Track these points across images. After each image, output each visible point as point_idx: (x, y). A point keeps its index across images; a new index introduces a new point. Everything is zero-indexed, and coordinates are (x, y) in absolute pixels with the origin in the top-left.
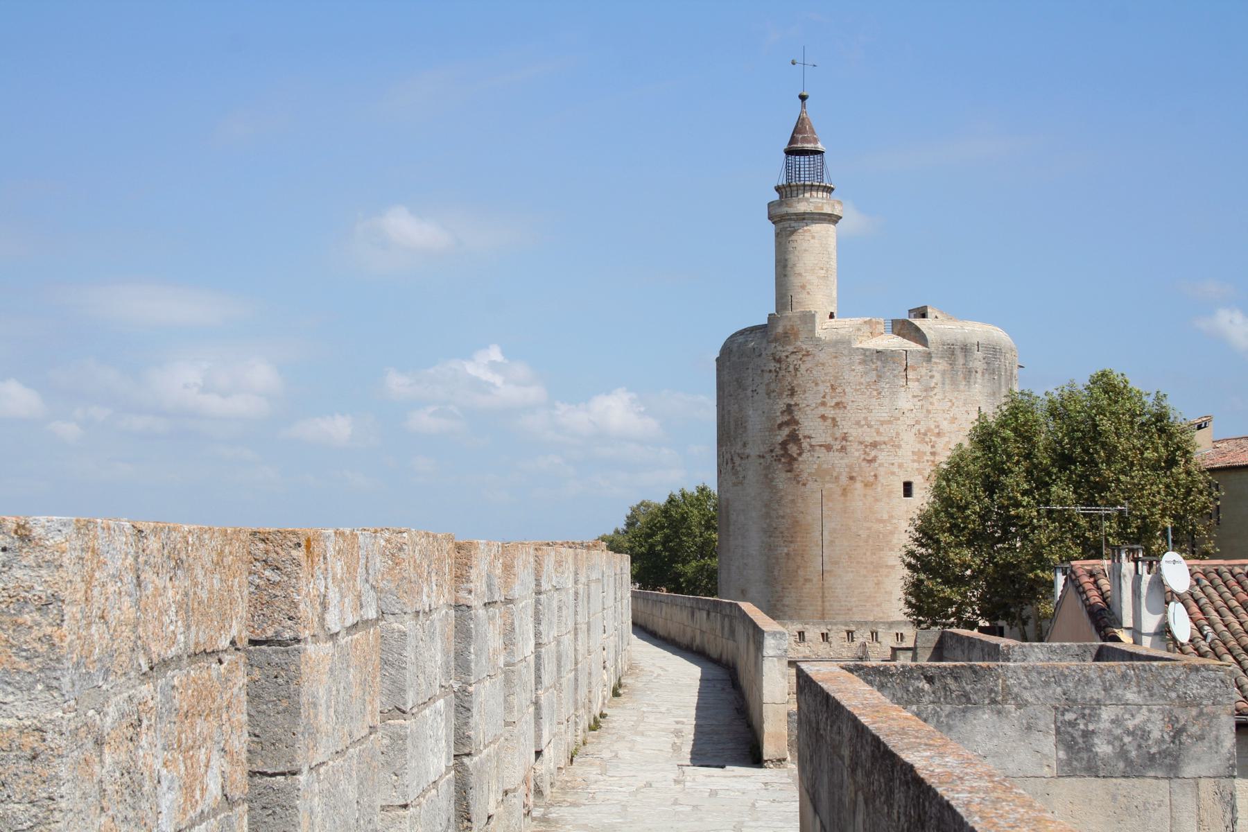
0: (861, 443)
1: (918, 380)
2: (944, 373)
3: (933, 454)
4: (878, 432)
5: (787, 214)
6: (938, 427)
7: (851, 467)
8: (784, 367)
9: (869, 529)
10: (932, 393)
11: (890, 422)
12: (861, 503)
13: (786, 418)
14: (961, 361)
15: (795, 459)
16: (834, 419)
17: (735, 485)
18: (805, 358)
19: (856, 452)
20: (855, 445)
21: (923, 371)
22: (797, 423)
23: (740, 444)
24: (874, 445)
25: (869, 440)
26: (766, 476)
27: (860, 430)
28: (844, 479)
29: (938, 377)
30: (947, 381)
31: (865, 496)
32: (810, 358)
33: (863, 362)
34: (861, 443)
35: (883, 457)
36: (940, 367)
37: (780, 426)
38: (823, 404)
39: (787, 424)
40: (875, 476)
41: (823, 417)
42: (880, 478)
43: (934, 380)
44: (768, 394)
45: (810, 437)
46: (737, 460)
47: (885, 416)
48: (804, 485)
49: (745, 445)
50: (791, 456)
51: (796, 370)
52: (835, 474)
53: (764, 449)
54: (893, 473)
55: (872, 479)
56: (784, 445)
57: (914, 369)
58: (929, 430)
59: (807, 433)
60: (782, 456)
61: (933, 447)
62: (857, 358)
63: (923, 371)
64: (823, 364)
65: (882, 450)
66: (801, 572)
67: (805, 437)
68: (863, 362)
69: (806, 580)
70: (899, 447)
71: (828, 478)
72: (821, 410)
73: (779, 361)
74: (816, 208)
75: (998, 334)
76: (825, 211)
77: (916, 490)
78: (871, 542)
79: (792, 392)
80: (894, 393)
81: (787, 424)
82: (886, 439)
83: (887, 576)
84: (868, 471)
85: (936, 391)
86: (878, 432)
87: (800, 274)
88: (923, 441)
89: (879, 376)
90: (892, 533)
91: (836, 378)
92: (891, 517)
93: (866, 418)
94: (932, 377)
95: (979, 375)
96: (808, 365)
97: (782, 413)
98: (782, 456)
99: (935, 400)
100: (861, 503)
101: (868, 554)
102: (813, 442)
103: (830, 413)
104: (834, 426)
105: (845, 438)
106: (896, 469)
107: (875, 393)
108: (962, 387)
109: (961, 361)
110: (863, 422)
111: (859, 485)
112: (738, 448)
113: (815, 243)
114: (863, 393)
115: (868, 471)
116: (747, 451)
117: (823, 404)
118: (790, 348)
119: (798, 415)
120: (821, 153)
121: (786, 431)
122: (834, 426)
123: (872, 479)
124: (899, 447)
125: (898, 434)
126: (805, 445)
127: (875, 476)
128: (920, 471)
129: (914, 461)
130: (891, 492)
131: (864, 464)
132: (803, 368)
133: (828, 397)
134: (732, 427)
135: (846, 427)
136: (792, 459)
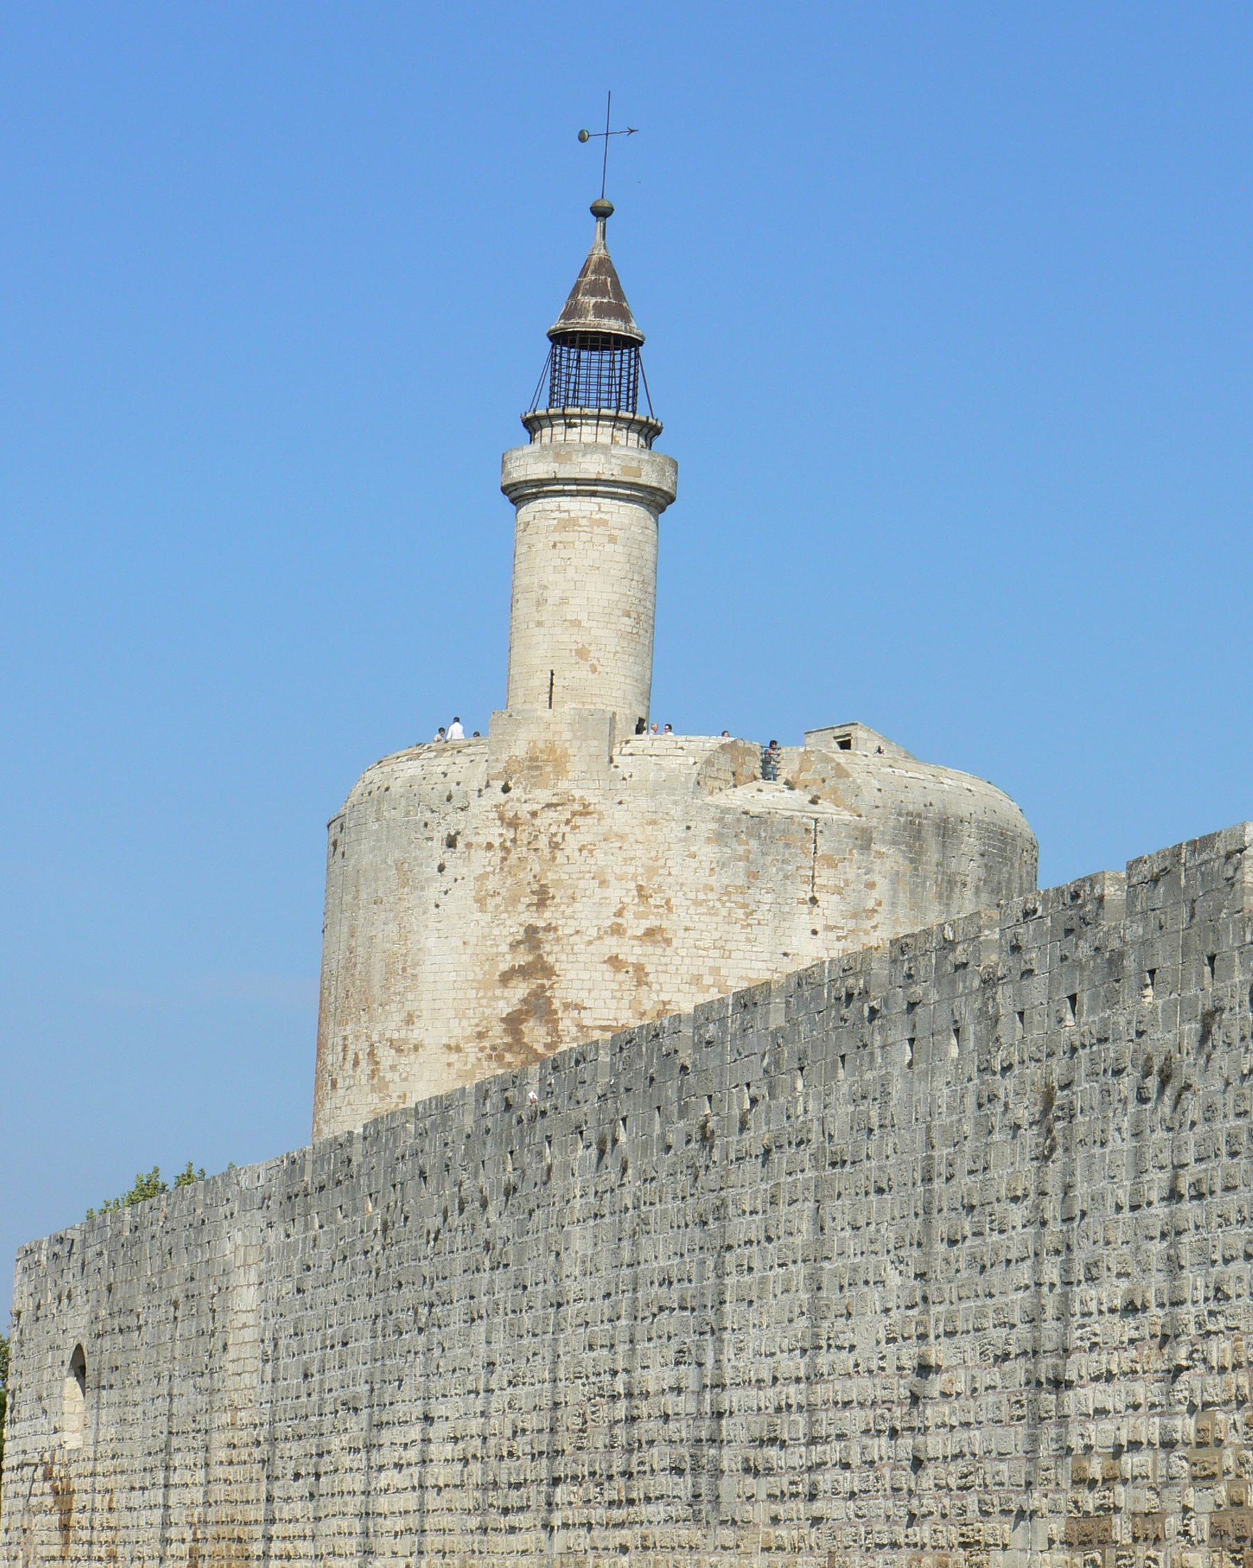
1: (839, 891)
2: (896, 878)
8: (523, 837)
10: (868, 924)
13: (523, 958)
14: (933, 855)
16: (639, 968)
18: (578, 821)
22: (548, 971)
23: (397, 1018)
29: (883, 885)
30: (903, 898)
32: (589, 820)
33: (718, 838)
36: (889, 864)
37: (506, 978)
39: (523, 972)
43: (875, 894)
44: (480, 901)
45: (579, 1007)
46: (386, 1056)
49: (409, 1020)
51: (554, 846)
53: (461, 1030)
56: (513, 1022)
59: (571, 997)
60: (509, 1048)
63: (852, 873)
64: (621, 837)
67: (567, 1006)
68: (718, 838)
72: (611, 945)
73: (514, 823)
74: (625, 469)
75: (1008, 809)
76: (643, 480)
79: (542, 899)
80: (783, 916)
81: (523, 972)
85: (877, 918)
89: (753, 875)
93: (715, 971)
94: (871, 885)
96: (586, 838)
97: (514, 946)
98: (509, 1048)
103: (631, 952)
104: (640, 983)
107: (740, 913)
112: (392, 1025)
114: (713, 912)
116: (416, 1034)
117: (617, 930)
118: (544, 796)
119: (552, 953)
120: (632, 343)
121: (520, 990)
122: (640, 983)
132: (572, 842)
133: (628, 915)
134: (377, 978)
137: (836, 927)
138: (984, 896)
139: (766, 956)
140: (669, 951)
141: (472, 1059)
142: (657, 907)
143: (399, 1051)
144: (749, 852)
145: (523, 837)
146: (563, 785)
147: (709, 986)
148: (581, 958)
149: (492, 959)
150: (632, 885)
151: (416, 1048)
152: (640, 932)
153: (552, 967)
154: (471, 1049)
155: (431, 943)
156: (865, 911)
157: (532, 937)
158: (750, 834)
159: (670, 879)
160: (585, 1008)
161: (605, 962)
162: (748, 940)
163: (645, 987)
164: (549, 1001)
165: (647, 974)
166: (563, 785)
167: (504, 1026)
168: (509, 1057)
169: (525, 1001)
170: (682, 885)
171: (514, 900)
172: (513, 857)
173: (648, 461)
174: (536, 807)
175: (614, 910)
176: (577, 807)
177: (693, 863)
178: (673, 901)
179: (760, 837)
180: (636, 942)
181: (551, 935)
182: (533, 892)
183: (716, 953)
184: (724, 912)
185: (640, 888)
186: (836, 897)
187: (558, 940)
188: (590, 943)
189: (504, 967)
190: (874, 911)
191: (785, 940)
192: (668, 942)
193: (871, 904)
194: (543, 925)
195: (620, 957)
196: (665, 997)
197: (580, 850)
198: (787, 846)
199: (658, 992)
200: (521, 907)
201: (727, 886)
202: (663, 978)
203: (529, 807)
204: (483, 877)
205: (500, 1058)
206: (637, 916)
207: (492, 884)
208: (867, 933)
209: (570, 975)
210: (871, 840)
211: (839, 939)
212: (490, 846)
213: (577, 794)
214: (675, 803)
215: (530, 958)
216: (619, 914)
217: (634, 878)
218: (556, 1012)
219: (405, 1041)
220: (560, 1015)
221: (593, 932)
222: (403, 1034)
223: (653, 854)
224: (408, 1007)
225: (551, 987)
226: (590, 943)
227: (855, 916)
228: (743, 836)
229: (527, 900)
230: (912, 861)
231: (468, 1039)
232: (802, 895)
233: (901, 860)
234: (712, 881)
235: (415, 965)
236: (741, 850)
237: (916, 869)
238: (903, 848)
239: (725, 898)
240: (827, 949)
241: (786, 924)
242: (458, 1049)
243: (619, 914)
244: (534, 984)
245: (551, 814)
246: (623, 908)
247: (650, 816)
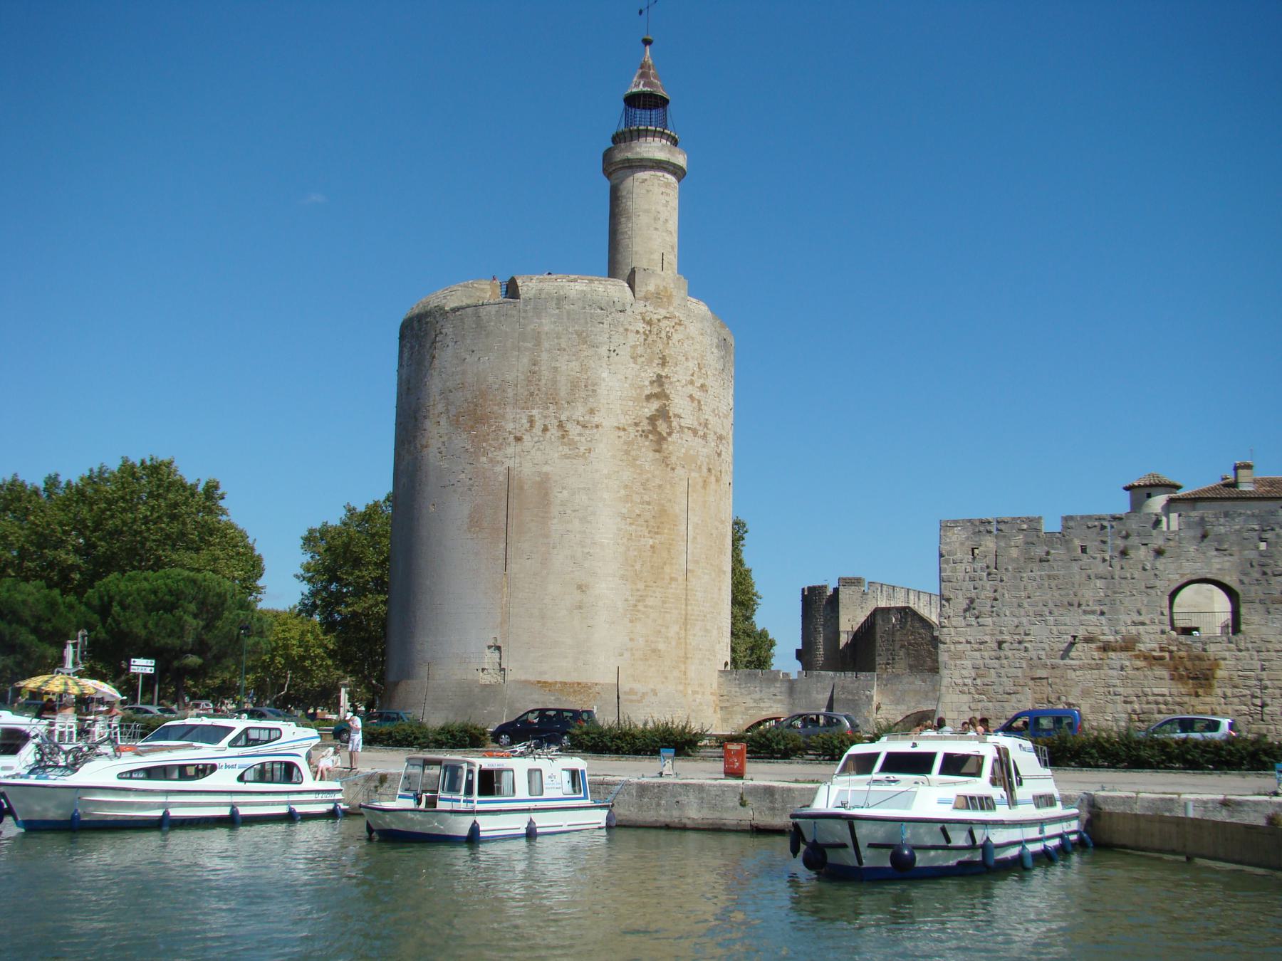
5: (628, 160)
8: (655, 331)
13: (656, 390)
15: (665, 439)
17: (566, 457)
18: (677, 327)
22: (667, 397)
26: (627, 453)
28: (705, 470)
32: (682, 328)
37: (648, 398)
38: (692, 382)
39: (656, 396)
41: (691, 396)
44: (634, 358)
46: (574, 430)
48: (673, 469)
49: (592, 411)
50: (660, 434)
51: (669, 338)
53: (624, 421)
56: (652, 420)
60: (650, 432)
66: (667, 569)
67: (675, 415)
73: (649, 323)
79: (664, 363)
81: (656, 396)
97: (652, 383)
98: (650, 432)
112: (579, 412)
116: (596, 419)
117: (692, 382)
118: (663, 312)
121: (655, 405)
126: (674, 424)
132: (675, 337)
136: (661, 439)
141: (632, 436)
143: (584, 427)
145: (655, 331)
146: (671, 309)
149: (641, 388)
151: (597, 427)
154: (631, 430)
155: (605, 375)
157: (659, 380)
166: (671, 309)
168: (651, 437)
171: (650, 361)
172: (650, 339)
189: (647, 392)
203: (656, 317)
204: (634, 347)
205: (647, 437)
206: (700, 378)
207: (640, 350)
212: (638, 332)
219: (589, 422)
222: (587, 418)
224: (590, 405)
231: (630, 425)
235: (595, 385)
242: (624, 430)
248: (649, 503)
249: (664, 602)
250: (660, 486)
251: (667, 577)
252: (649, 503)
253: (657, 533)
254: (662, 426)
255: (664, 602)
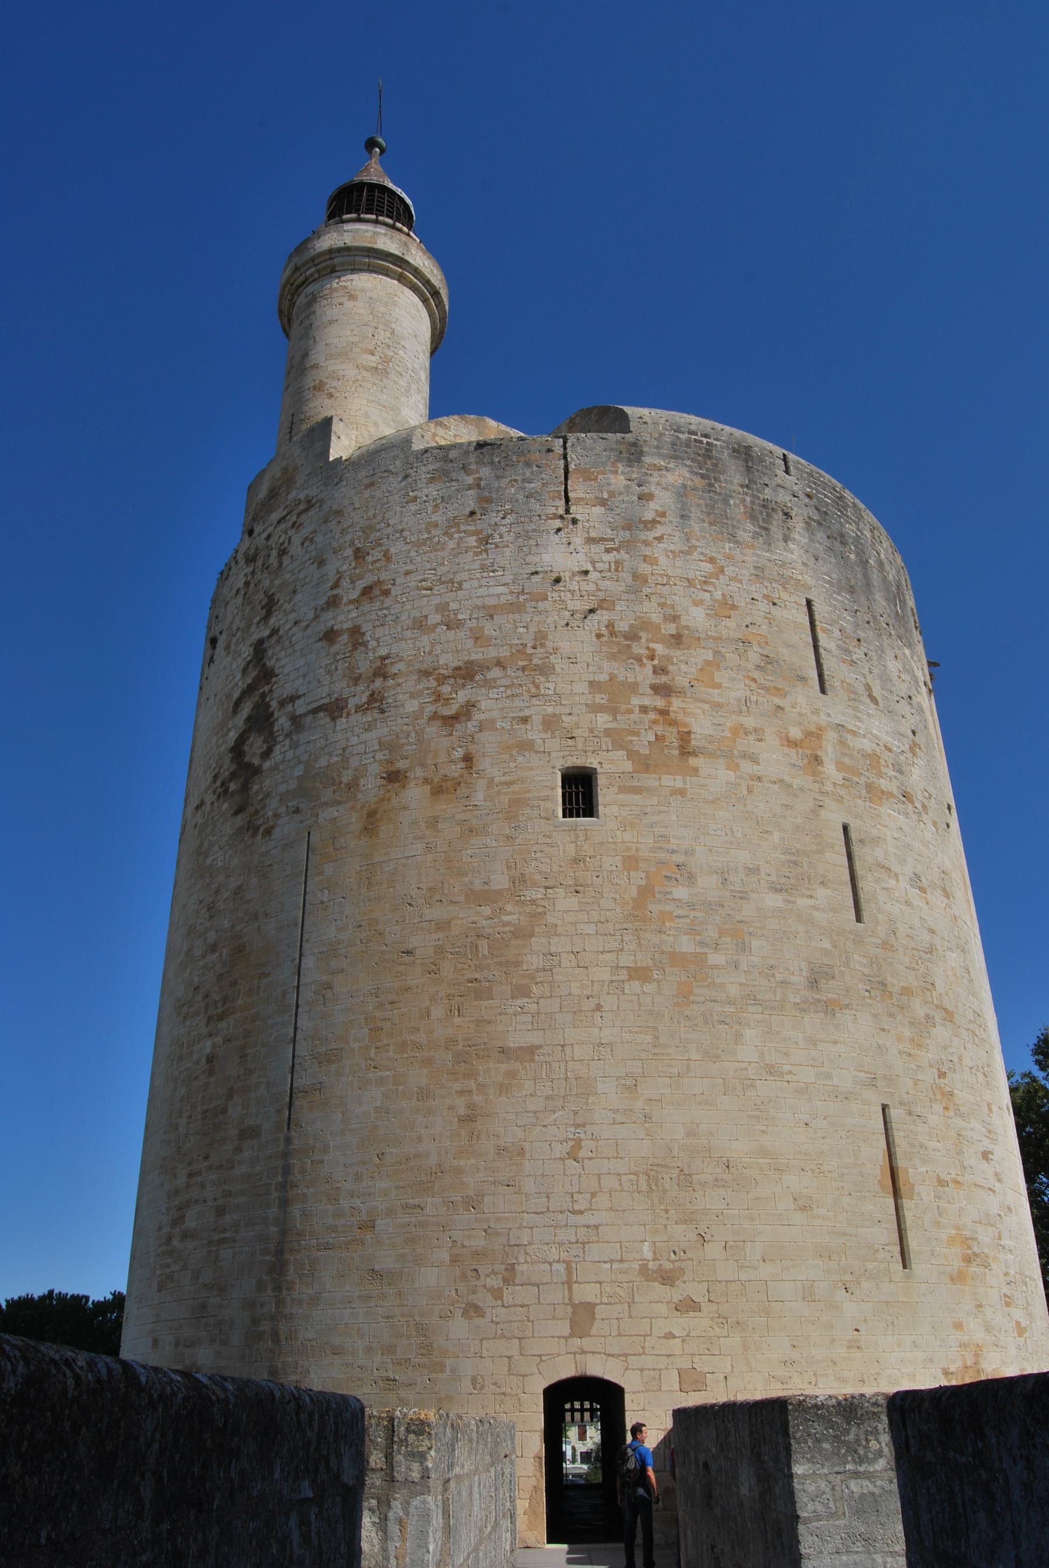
0: (426, 674)
1: (603, 503)
2: (682, 493)
3: (663, 690)
4: (478, 638)
6: (675, 618)
7: (391, 746)
9: (443, 926)
10: (651, 535)
11: (515, 608)
12: (419, 848)
15: (257, 771)
16: (356, 631)
18: (303, 517)
19: (409, 700)
20: (410, 684)
21: (618, 481)
24: (467, 673)
25: (448, 660)
27: (425, 641)
28: (371, 784)
29: (663, 500)
30: (695, 513)
31: (434, 822)
33: (440, 476)
34: (426, 674)
35: (490, 704)
37: (238, 703)
40: (468, 759)
42: (484, 764)
43: (653, 505)
47: (498, 592)
48: (268, 832)
50: (249, 765)
51: (283, 552)
52: (346, 777)
54: (526, 746)
55: (455, 770)
57: (588, 476)
58: (645, 625)
59: (287, 691)
61: (660, 670)
62: (423, 472)
65: (488, 684)
69: (248, 1133)
70: (546, 670)
71: (327, 794)
77: (605, 795)
78: (447, 969)
79: (270, 606)
82: (504, 653)
83: (503, 1088)
84: (445, 748)
85: (659, 531)
86: (478, 638)
87: (316, 366)
88: (624, 654)
90: (522, 934)
91: (368, 530)
92: (520, 881)
93: (442, 608)
95: (798, 525)
96: (305, 532)
97: (244, 671)
99: (658, 551)
100: (419, 848)
101: (438, 1012)
102: (300, 707)
103: (343, 619)
104: (355, 648)
105: (381, 672)
106: (534, 733)
107: (472, 541)
108: (744, 536)
109: (734, 477)
110: (435, 618)
111: (415, 794)
113: (358, 308)
115: (445, 748)
123: (455, 770)
124: (546, 670)
125: (541, 638)
127: (468, 759)
128: (618, 739)
129: (595, 709)
130: (517, 803)
131: (433, 730)
132: (296, 540)
133: (345, 583)
135: (383, 641)
137: (602, 539)
138: (820, 535)
139: (508, 578)
140: (388, 602)
142: (375, 562)
144: (480, 479)
147: (436, 626)
148: (298, 647)
150: (349, 552)
152: (355, 595)
153: (273, 670)
156: (641, 521)
158: (480, 462)
159: (390, 530)
160: (299, 697)
161: (320, 640)
162: (483, 568)
163: (363, 649)
164: (268, 705)
165: (363, 634)
166: (292, 496)
167: (231, 755)
169: (249, 719)
170: (402, 531)
173: (385, 235)
174: (270, 530)
175: (330, 585)
176: (302, 507)
177: (413, 507)
178: (392, 550)
179: (492, 463)
180: (352, 607)
181: (275, 638)
182: (262, 609)
183: (442, 589)
184: (452, 544)
185: (357, 551)
186: (598, 510)
187: (281, 637)
188: (307, 627)
190: (654, 522)
191: (529, 559)
192: (386, 593)
193: (649, 516)
194: (267, 632)
195: (335, 628)
196: (383, 652)
197: (302, 544)
198: (528, 464)
199: (374, 650)
200: (253, 628)
201: (455, 518)
202: (379, 632)
203: (265, 535)
205: (226, 791)
208: (646, 543)
209: (286, 670)
210: (641, 453)
211: (608, 551)
213: (302, 496)
214: (395, 458)
215: (256, 673)
216: (336, 585)
217: (352, 542)
218: (273, 713)
220: (276, 715)
221: (311, 615)
223: (371, 514)
225: (271, 691)
226: (307, 627)
227: (628, 527)
228: (473, 467)
229: (255, 621)
230: (703, 476)
232: (553, 510)
233: (687, 475)
234: (435, 518)
236: (470, 480)
237: (711, 485)
238: (688, 463)
239: (453, 530)
240: (593, 563)
241: (532, 542)
243: (336, 585)
244: (255, 698)
245: (282, 527)
246: (340, 578)
247: (367, 481)
248: (213, 948)
249: (220, 1211)
250: (239, 891)
251: (233, 1132)
252: (213, 948)
253: (221, 1017)
254: (256, 744)
255: (220, 1211)
